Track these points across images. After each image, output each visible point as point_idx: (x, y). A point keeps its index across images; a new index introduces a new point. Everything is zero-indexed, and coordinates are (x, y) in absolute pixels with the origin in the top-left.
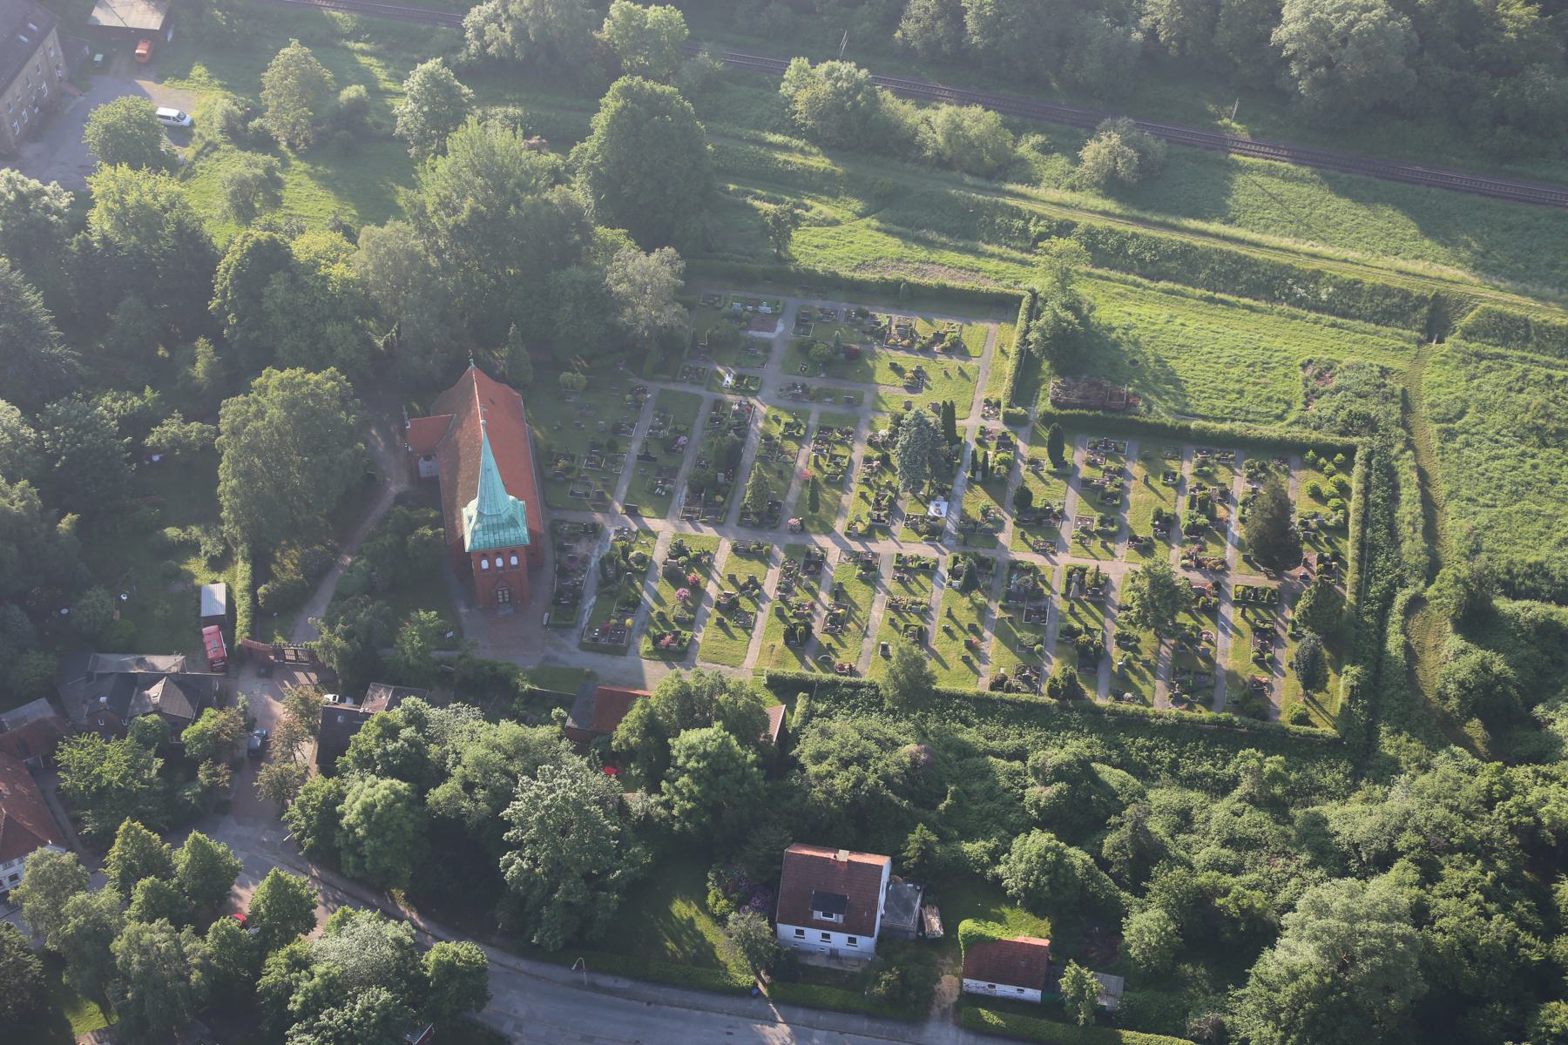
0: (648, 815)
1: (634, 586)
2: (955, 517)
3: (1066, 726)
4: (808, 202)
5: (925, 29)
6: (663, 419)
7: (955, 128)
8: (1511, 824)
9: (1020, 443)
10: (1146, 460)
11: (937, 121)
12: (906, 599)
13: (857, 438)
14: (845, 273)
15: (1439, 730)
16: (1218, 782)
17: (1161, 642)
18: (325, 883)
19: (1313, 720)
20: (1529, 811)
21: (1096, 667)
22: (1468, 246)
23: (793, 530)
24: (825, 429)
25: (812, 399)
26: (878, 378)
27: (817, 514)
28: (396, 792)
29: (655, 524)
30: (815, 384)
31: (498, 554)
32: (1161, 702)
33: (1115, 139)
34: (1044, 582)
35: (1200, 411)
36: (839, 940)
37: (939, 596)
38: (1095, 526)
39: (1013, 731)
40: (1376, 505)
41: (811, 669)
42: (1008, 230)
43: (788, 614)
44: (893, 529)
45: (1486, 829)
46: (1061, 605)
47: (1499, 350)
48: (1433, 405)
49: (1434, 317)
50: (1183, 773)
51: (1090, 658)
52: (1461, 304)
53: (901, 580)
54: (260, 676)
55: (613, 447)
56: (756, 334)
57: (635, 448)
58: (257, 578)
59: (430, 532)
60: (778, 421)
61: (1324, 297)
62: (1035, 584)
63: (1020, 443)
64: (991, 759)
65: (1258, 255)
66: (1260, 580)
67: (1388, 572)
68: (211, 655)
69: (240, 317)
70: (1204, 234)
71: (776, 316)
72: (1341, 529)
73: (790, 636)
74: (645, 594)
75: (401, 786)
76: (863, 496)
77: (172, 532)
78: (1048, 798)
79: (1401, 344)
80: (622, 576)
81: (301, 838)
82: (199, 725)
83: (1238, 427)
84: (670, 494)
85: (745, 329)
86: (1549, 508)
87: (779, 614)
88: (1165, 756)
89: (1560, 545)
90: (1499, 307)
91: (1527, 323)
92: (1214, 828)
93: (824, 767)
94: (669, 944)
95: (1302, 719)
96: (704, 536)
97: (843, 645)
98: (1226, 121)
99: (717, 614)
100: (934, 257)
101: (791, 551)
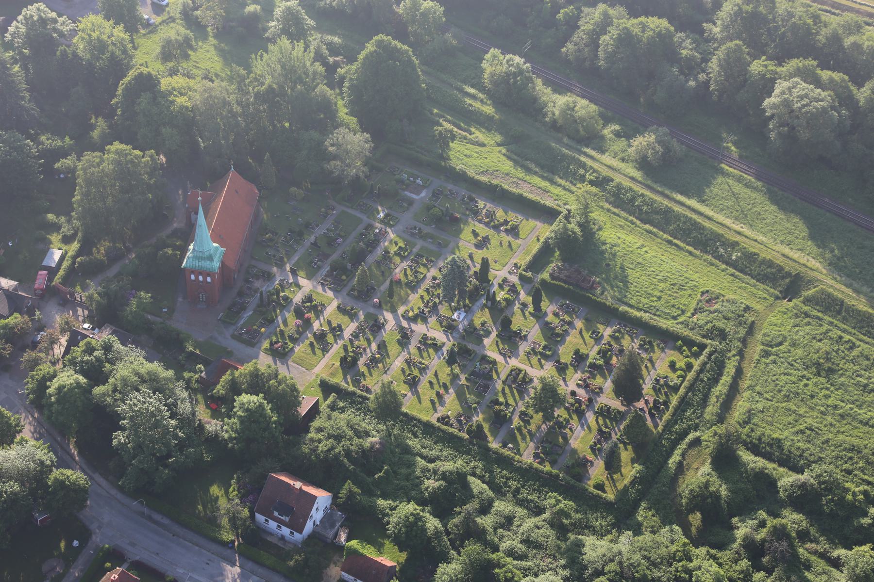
0: (217, 435)
1: (275, 311)
2: (466, 323)
3: (468, 453)
4: (473, 130)
5: (579, 51)
7: (570, 109)
8: (676, 575)
9: (522, 292)
10: (588, 321)
11: (557, 103)
12: (417, 359)
13: (434, 265)
14: (471, 173)
15: (671, 513)
16: (536, 507)
17: (544, 422)
18: (39, 422)
19: (606, 489)
20: (690, 572)
21: (501, 425)
22: (832, 251)
24: (419, 256)
25: (421, 237)
26: (462, 236)
27: (391, 301)
28: (78, 383)
29: (303, 281)
30: (427, 229)
31: (201, 273)
32: (527, 456)
33: (653, 138)
34: (497, 372)
35: (632, 302)
36: (285, 531)
37: (436, 363)
38: (540, 349)
39: (438, 447)
40: (702, 381)
41: (347, 383)
42: (575, 174)
44: (429, 320)
45: (659, 574)
46: (499, 386)
47: (820, 315)
48: (765, 335)
49: (789, 284)
50: (520, 496)
51: (499, 420)
52: (810, 282)
53: (419, 348)
54: (60, 304)
55: (301, 234)
57: (312, 239)
58: (79, 253)
59: (170, 252)
60: (396, 244)
61: (734, 258)
62: (491, 371)
63: (522, 292)
64: (418, 458)
65: (707, 224)
66: (616, 404)
67: (691, 420)
68: (36, 286)
69: (123, 112)
70: (682, 204)
72: (676, 389)
73: (343, 360)
74: (279, 318)
75: (82, 380)
76: (422, 297)
77: (50, 217)
78: (433, 488)
79: (765, 295)
80: (272, 304)
81: (29, 394)
82: (7, 321)
83: (646, 316)
84: (319, 268)
85: (404, 190)
86: (801, 411)
87: (345, 348)
88: (514, 484)
89: (797, 433)
90: (831, 290)
91: (842, 302)
92: (521, 531)
93: (320, 436)
95: (600, 487)
97: (371, 375)
98: (730, 145)
99: (312, 339)
100: (527, 178)
101: (368, 316)
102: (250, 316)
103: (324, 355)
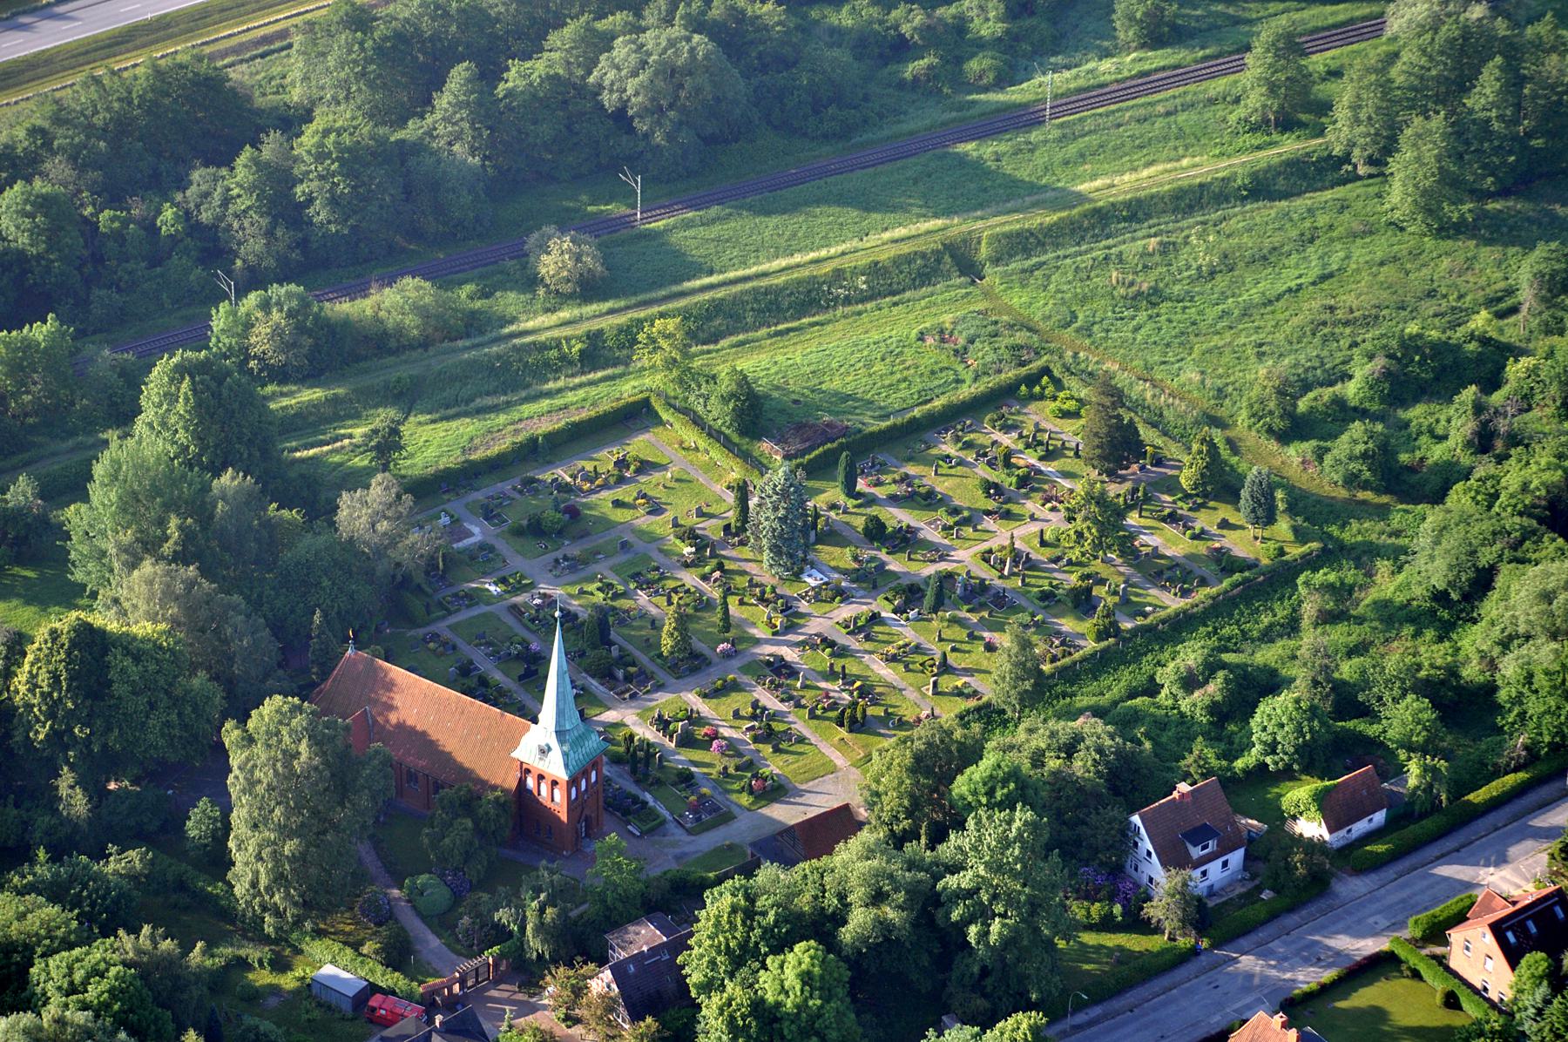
6: (489, 644)
10: (910, 459)
11: (394, 302)
23: (727, 655)
29: (610, 716)
30: (575, 551)
37: (907, 632)
39: (1106, 680)
43: (819, 712)
53: (868, 638)
56: (460, 544)
71: (455, 521)
76: (742, 603)
87: (813, 716)
94: (1086, 967)
96: (664, 702)
102: (656, 799)
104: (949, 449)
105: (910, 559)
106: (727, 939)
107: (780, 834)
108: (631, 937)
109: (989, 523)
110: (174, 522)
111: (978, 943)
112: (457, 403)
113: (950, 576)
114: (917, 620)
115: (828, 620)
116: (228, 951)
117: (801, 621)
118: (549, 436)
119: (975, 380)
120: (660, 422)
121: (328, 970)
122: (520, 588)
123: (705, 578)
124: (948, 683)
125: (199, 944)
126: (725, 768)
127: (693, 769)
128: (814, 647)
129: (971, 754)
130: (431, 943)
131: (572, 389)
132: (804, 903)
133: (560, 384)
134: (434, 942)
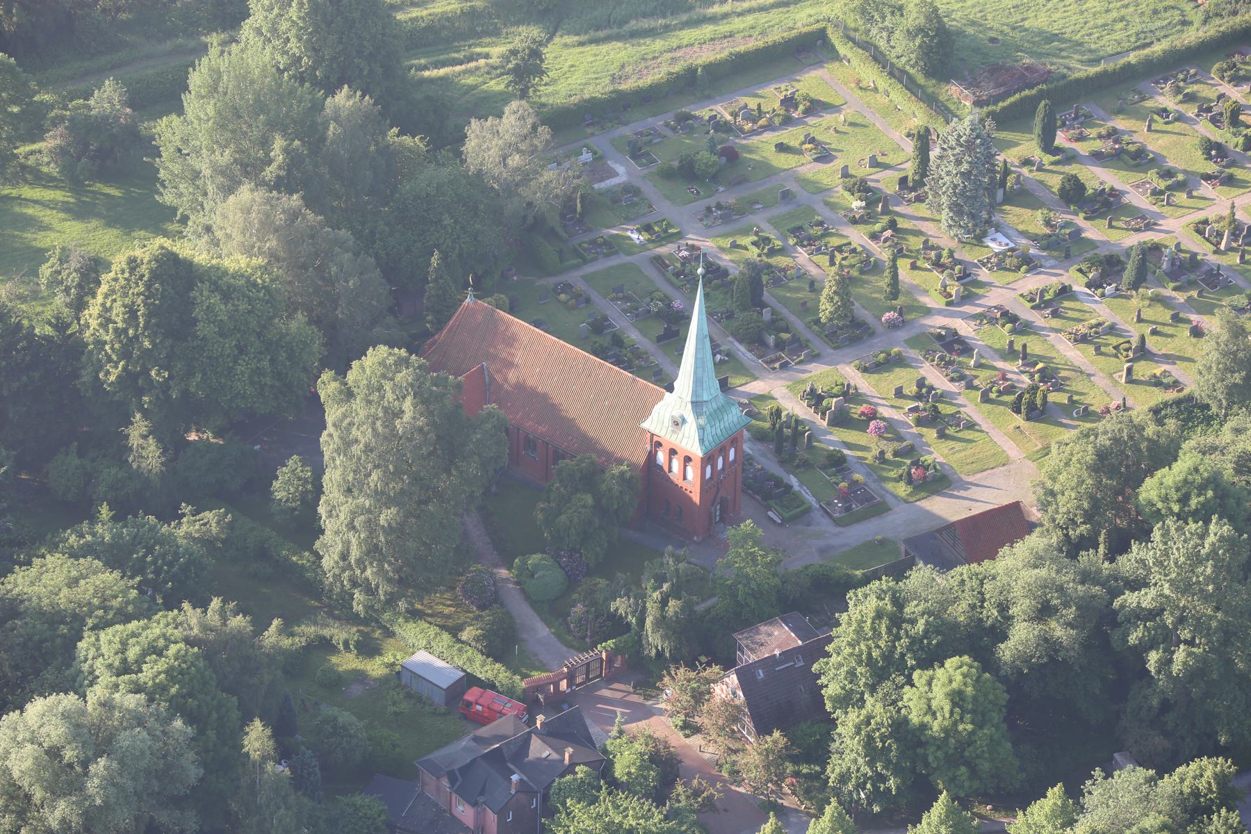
10: (1120, 111)
29: (757, 387)
30: (729, 198)
35: (1109, 50)
37: (1102, 310)
43: (993, 396)
53: (1055, 314)
71: (599, 158)
76: (914, 267)
87: (986, 399)
96: (820, 374)
102: (801, 483)
103: (982, 431)
104: (1166, 100)
105: (1111, 226)
106: (869, 648)
107: (939, 531)
108: (762, 638)
109: (1206, 189)
110: (278, 143)
111: (1159, 672)
112: (609, 24)
113: (1156, 248)
114: (1114, 296)
115: (1010, 291)
116: (310, 630)
117: (980, 291)
118: (710, 68)
119: (1205, 22)
120: (836, 57)
121: (422, 656)
122: (665, 238)
123: (874, 237)
124: (1144, 370)
125: (276, 622)
126: (882, 453)
127: (846, 452)
128: (993, 321)
129: (1164, 455)
130: (540, 631)
131: (740, 15)
132: (959, 612)
133: (727, 8)
134: (543, 631)
